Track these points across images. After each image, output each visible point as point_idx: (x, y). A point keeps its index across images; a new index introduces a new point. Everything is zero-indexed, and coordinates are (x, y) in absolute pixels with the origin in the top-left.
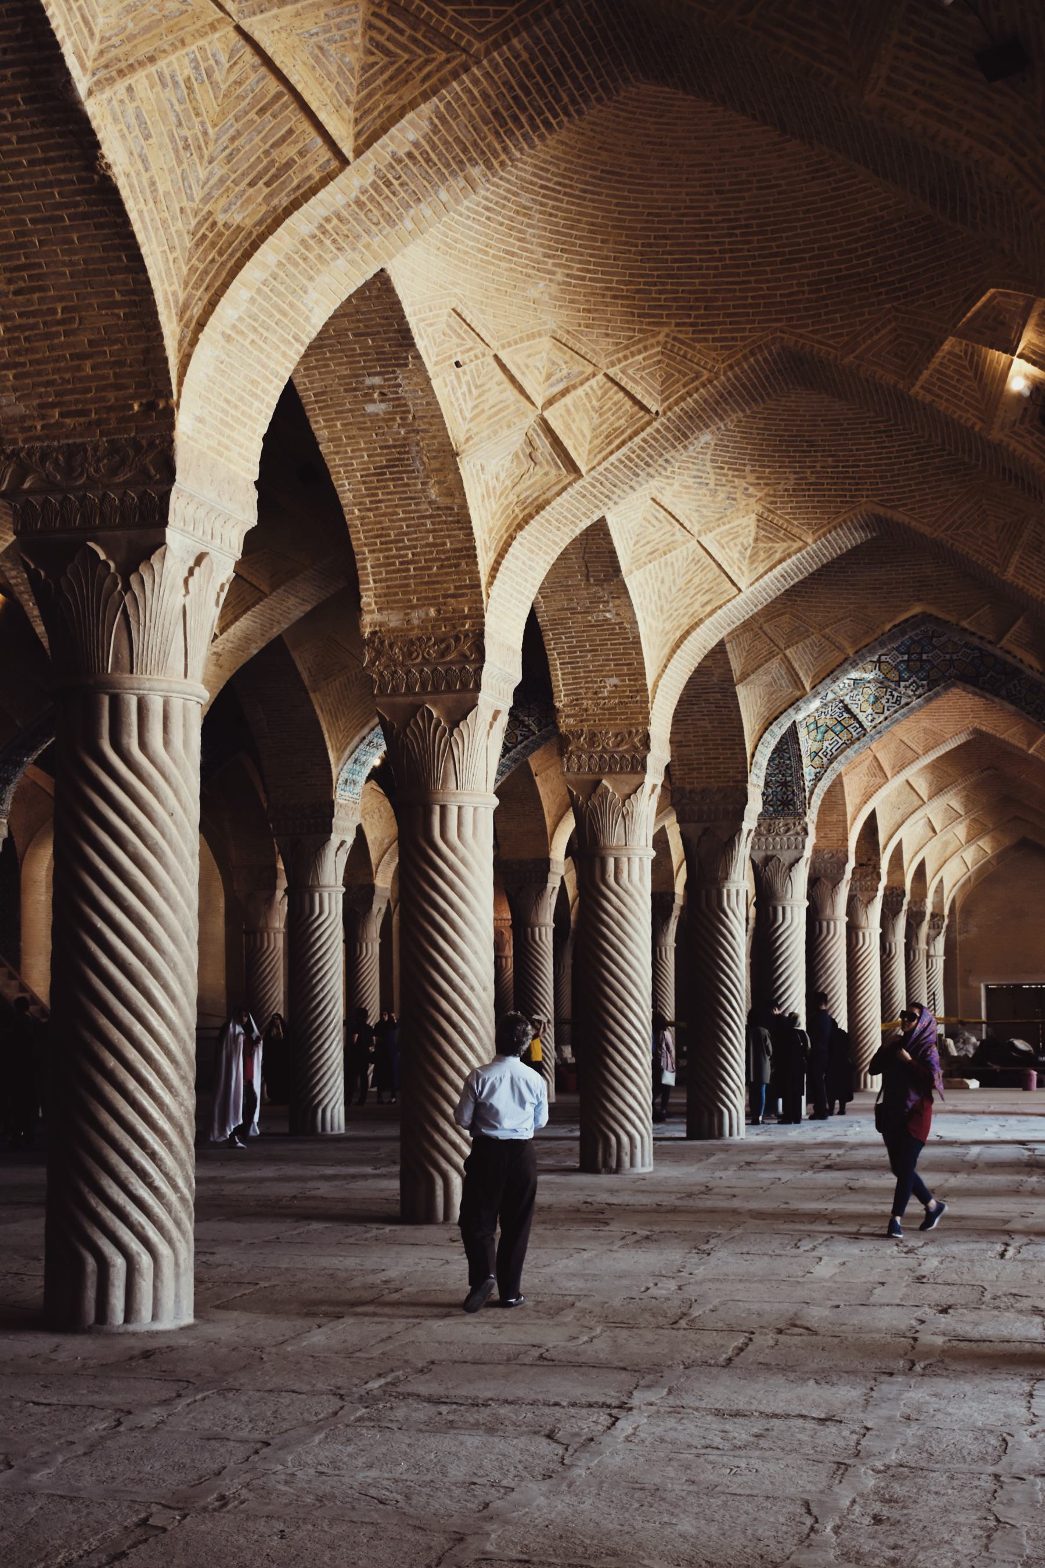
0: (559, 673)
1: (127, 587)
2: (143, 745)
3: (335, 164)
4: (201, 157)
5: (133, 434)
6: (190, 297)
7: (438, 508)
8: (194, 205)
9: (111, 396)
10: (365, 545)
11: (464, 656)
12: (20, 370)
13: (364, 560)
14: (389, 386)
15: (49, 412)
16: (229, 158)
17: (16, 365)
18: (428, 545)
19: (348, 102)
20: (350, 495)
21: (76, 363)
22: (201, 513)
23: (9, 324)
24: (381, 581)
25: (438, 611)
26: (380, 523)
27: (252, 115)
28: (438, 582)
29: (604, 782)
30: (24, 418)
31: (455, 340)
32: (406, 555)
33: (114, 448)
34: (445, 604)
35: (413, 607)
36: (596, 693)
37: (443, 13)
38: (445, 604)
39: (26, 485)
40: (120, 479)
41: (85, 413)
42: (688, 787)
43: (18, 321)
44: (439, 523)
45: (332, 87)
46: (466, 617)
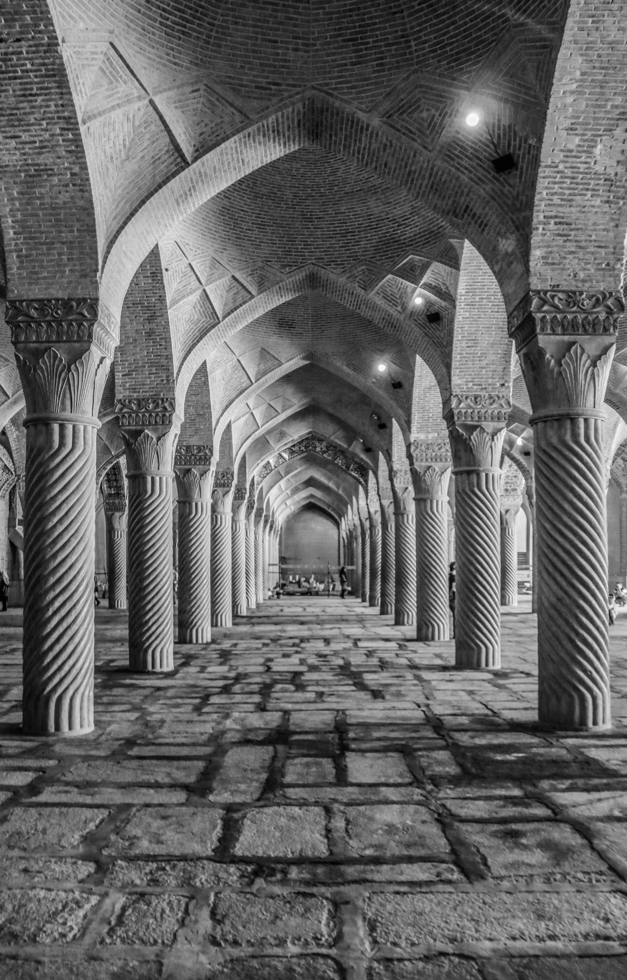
30: (460, 385)
33: (490, 397)
40: (493, 407)
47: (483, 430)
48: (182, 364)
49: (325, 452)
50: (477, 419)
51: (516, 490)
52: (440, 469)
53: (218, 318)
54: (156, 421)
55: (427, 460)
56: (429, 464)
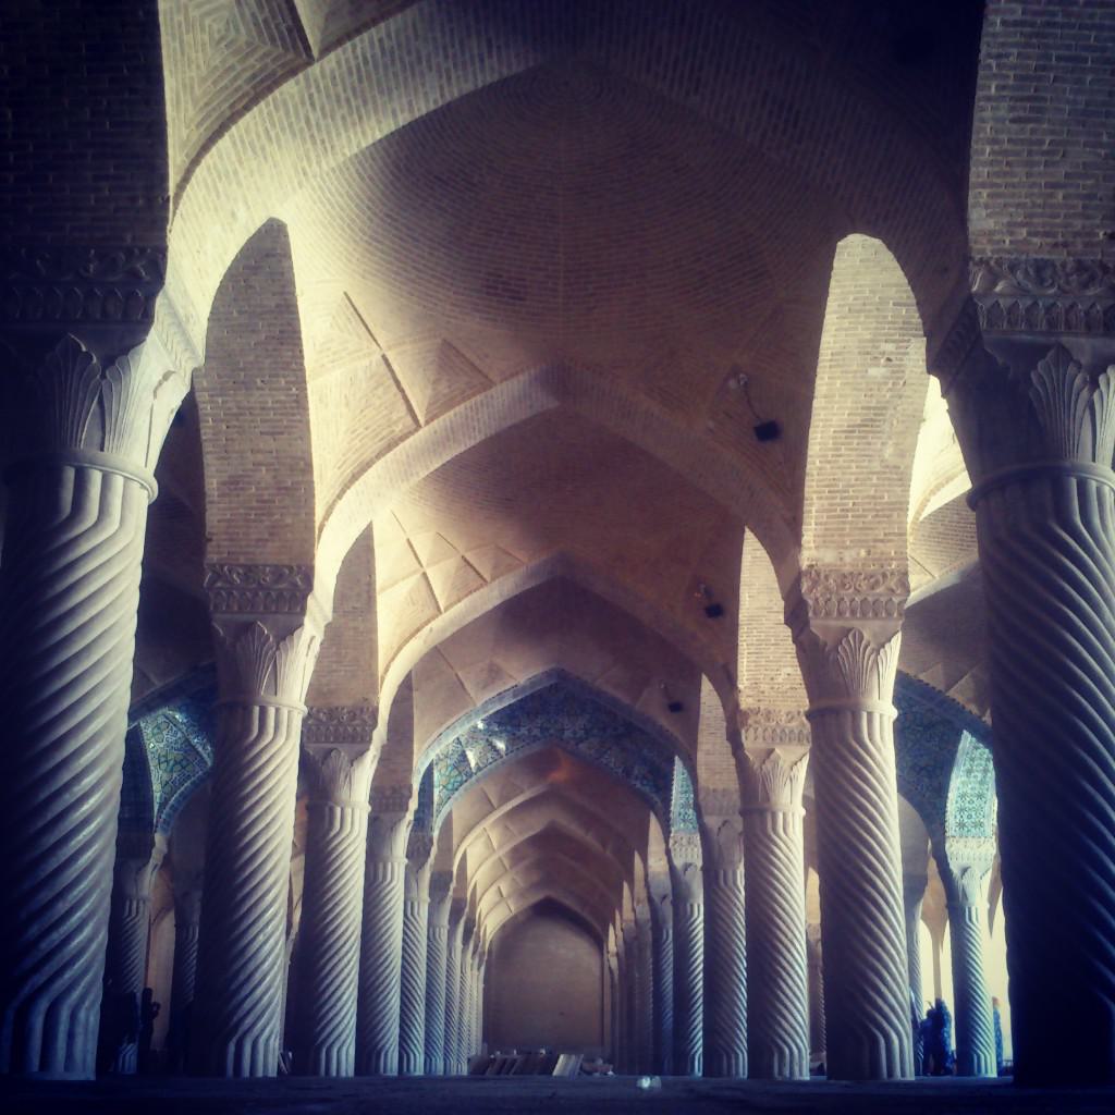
0: (745, 660)
5: (1099, 257)
7: (887, 467)
9: (1078, 224)
10: (815, 492)
11: (893, 591)
12: (994, 190)
13: (811, 505)
14: (898, 354)
15: (1017, 230)
17: (993, 185)
18: (868, 497)
20: (818, 447)
21: (1049, 191)
23: (996, 147)
24: (821, 524)
26: (834, 474)
28: (872, 529)
29: (778, 751)
30: (992, 233)
32: (848, 504)
33: (1081, 267)
34: (874, 547)
35: (847, 548)
36: (772, 679)
38: (874, 547)
39: (998, 289)
40: (1091, 292)
41: (1054, 235)
42: (711, 787)
43: (1006, 146)
44: (884, 479)
46: (892, 559)
47: (1065, 355)
48: (195, 162)
49: (581, 740)
50: (1044, 327)
51: (981, 824)
52: (875, 635)
53: (307, 48)
54: (104, 313)
55: (840, 613)
56: (847, 624)
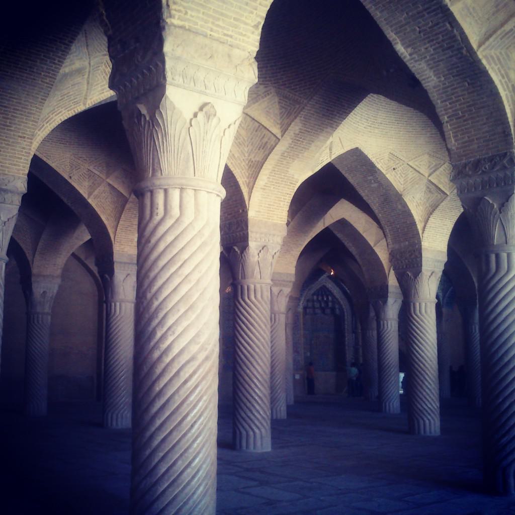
1: (242, 257)
2: (249, 298)
3: (277, 140)
4: (245, 146)
6: (250, 181)
8: (246, 158)
16: (252, 144)
19: (278, 123)
22: (263, 235)
25: (409, 242)
27: (254, 132)
31: (392, 162)
37: (295, 95)
45: (272, 121)
